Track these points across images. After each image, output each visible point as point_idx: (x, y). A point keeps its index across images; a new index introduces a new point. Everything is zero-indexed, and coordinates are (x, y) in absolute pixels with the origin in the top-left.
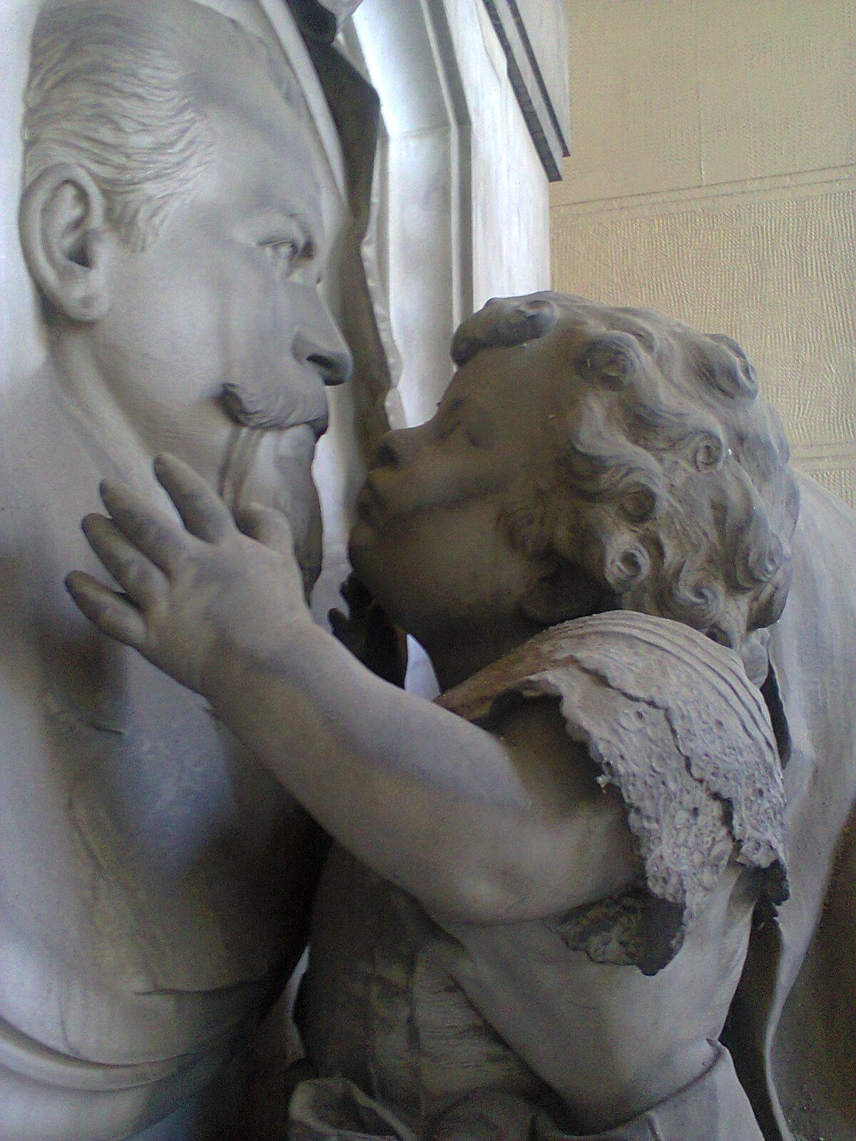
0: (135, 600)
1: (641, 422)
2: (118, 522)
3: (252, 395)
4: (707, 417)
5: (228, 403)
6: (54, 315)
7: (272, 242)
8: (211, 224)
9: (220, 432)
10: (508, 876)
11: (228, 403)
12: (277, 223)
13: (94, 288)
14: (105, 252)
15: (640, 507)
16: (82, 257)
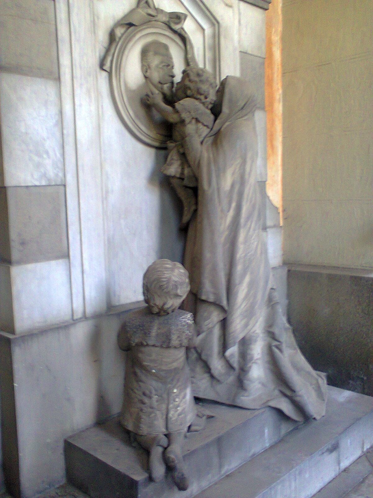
0: (148, 100)
1: (190, 81)
2: (147, 95)
3: (162, 82)
4: (197, 79)
5: (160, 83)
6: (146, 77)
7: (164, 66)
8: (157, 66)
9: (160, 85)
10: (172, 118)
11: (160, 83)
12: (164, 64)
13: (148, 74)
14: (149, 71)
15: (190, 88)
16: (146, 72)
